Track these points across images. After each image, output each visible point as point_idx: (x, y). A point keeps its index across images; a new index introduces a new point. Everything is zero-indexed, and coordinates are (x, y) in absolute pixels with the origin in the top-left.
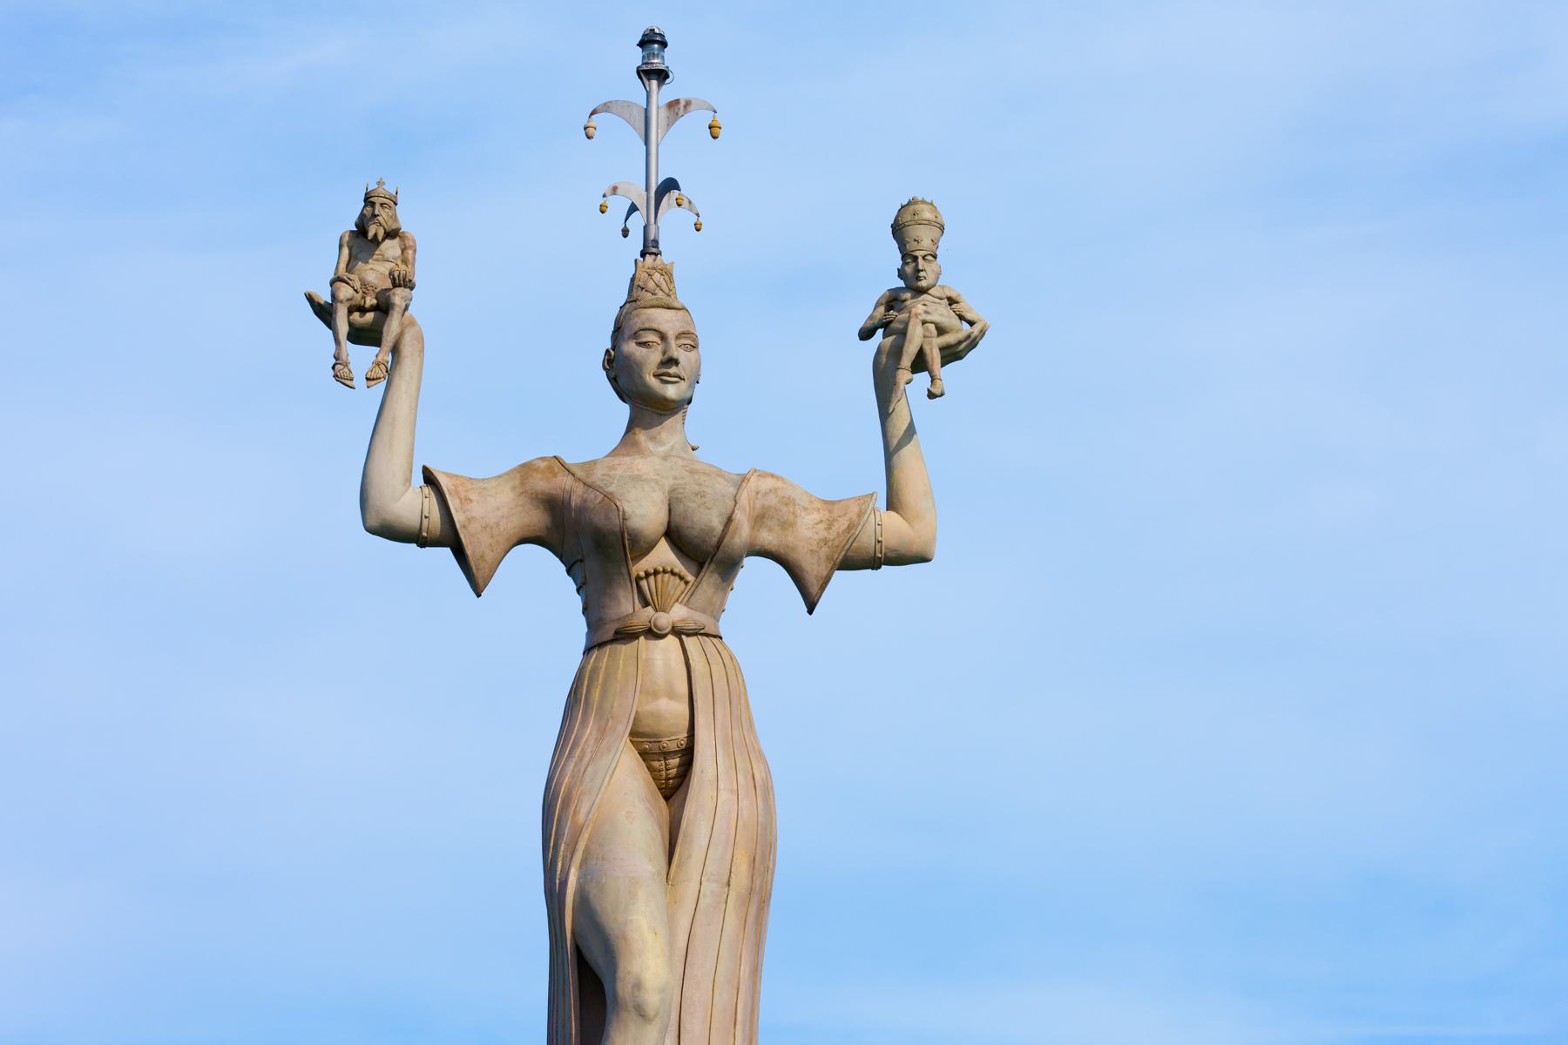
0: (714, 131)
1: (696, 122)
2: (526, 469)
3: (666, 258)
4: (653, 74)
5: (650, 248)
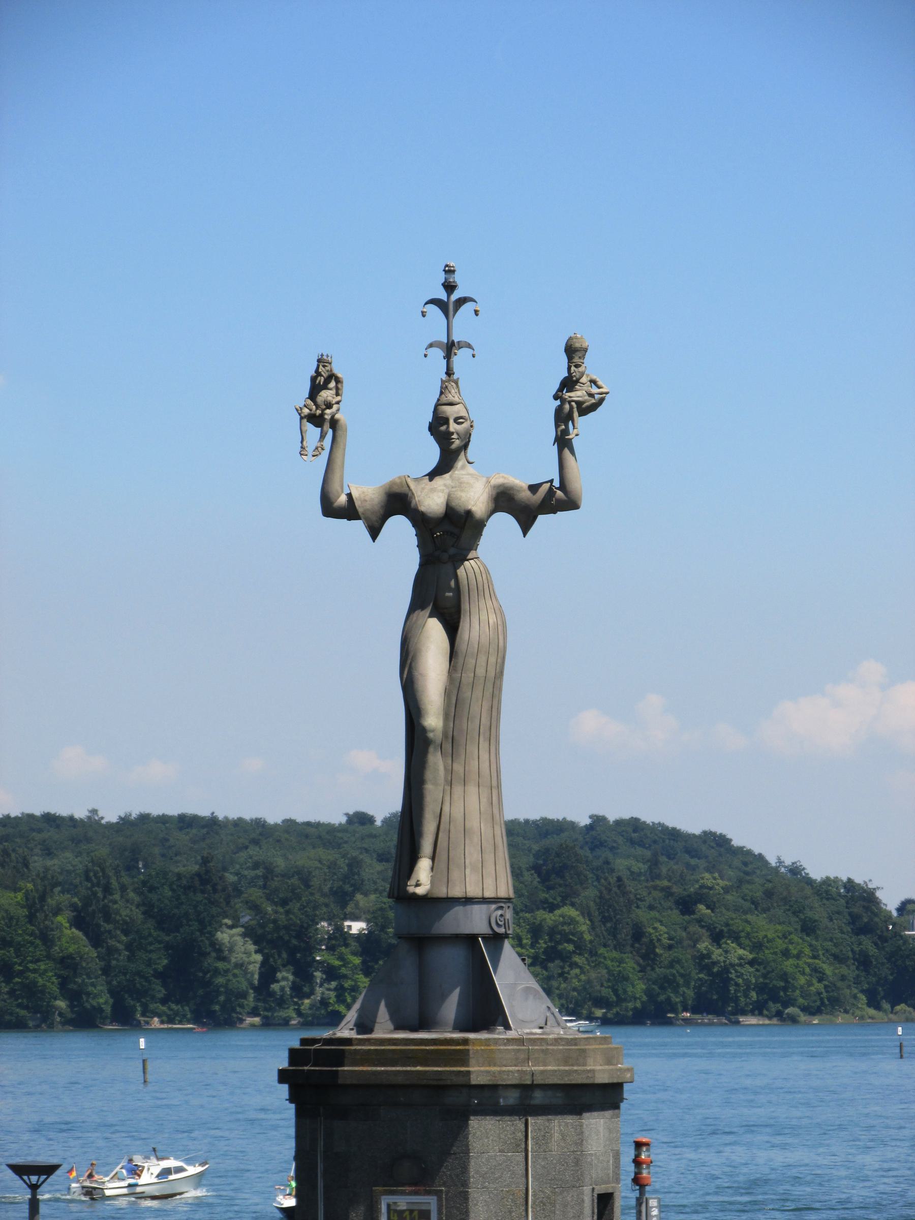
0: (476, 312)
1: (467, 308)
2: (392, 483)
3: (455, 377)
4: (450, 287)
5: (449, 372)
